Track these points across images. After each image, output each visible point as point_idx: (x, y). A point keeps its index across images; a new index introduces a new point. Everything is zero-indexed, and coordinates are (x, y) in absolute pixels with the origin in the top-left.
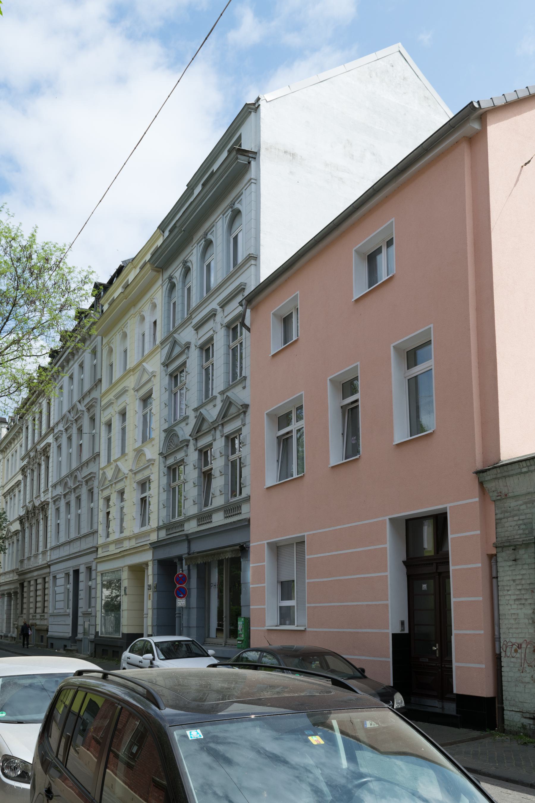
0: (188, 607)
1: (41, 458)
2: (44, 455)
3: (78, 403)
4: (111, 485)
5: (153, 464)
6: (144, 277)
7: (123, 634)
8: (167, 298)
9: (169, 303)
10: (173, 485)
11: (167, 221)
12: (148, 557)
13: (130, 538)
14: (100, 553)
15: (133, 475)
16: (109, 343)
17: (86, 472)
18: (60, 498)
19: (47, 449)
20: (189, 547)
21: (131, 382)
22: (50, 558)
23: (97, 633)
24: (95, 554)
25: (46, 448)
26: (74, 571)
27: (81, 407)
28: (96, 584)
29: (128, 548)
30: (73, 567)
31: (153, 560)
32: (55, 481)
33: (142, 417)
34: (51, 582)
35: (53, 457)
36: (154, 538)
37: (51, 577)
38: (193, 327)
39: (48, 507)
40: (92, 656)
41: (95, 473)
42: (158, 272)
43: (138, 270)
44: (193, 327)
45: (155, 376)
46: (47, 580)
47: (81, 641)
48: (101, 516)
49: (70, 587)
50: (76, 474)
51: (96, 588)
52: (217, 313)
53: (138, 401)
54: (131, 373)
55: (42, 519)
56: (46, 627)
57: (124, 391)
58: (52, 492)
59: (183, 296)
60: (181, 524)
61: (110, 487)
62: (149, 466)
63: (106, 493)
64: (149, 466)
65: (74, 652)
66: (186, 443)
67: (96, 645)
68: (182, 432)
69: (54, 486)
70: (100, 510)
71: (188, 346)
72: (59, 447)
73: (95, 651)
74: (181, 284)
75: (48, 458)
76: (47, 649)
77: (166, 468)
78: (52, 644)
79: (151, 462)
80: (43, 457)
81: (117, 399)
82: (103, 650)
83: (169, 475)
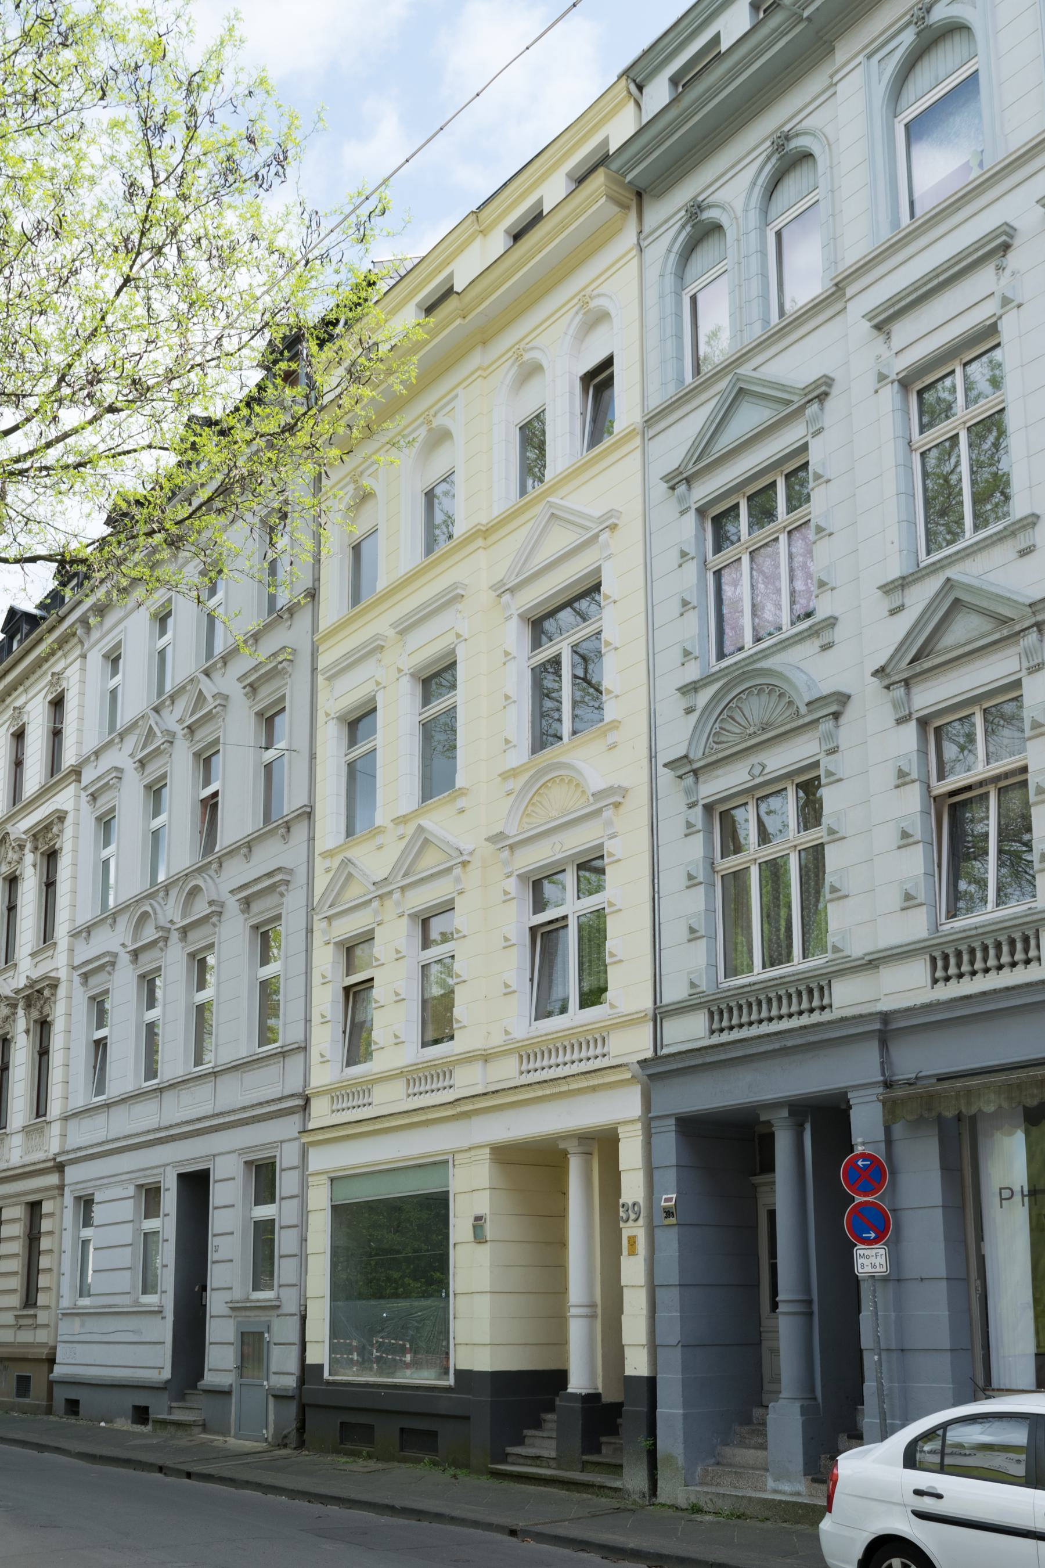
0: (894, 1278)
1: (20, 861)
2: (36, 848)
3: (203, 677)
4: (380, 897)
5: (617, 805)
6: (565, 228)
7: (458, 1373)
8: (670, 280)
9: (678, 295)
10: (733, 863)
11: (663, 50)
12: (622, 1108)
13: (486, 1057)
14: (321, 1113)
15: (506, 853)
16: (354, 478)
17: (239, 872)
18: (113, 964)
19: (55, 830)
20: (885, 1063)
21: (478, 571)
22: (63, 1143)
23: (308, 1373)
24: (297, 1118)
25: (48, 828)
26: (181, 1176)
27: (228, 682)
28: (304, 1213)
29: (479, 1090)
30: (176, 1164)
31: (649, 1122)
32: (85, 916)
33: (528, 675)
34: (69, 1215)
35: (75, 851)
36: (635, 1044)
37: (69, 1199)
38: (869, 316)
39: (54, 995)
40: (285, 1446)
41: (291, 872)
42: (625, 207)
43: (497, 242)
44: (869, 316)
45: (613, 527)
46: (47, 1207)
47: (225, 1393)
48: (327, 1000)
49: (166, 1225)
50: (200, 882)
51: (302, 1226)
52: (1016, 242)
53: (515, 622)
54: (480, 542)
55: (27, 1032)
56: (46, 1351)
57: (452, 598)
58: (71, 950)
59: (763, 253)
60: (815, 989)
61: (375, 904)
62: (598, 812)
63: (348, 927)
64: (598, 812)
65: (196, 1430)
66: (836, 705)
67: (302, 1409)
68: (804, 677)
69: (86, 932)
70: (316, 979)
71: (820, 393)
72: (106, 823)
73: (301, 1429)
74: (754, 216)
75: (51, 856)
76: (52, 1418)
77: (699, 810)
78: (73, 1406)
79: (613, 797)
80: (29, 858)
81: (401, 633)
82: (341, 1423)
83: (709, 831)
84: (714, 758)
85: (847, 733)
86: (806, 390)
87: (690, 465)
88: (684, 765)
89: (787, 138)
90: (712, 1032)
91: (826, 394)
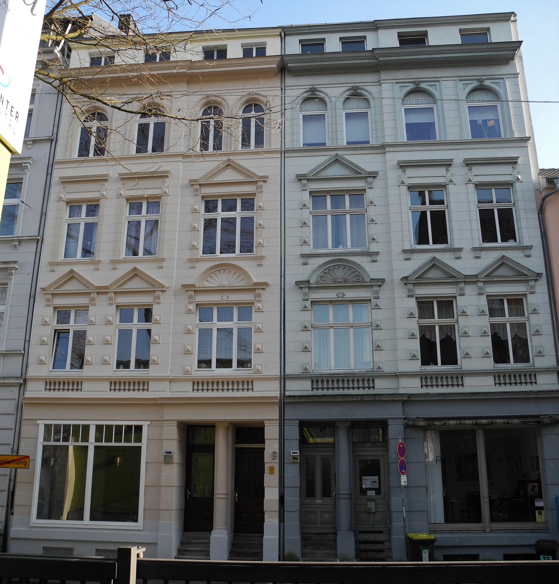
71: (374, 175)
84: (319, 285)
85: (384, 293)
86: (370, 173)
87: (311, 175)
88: (306, 284)
89: (358, 88)
90: (313, 389)
91: (375, 177)
